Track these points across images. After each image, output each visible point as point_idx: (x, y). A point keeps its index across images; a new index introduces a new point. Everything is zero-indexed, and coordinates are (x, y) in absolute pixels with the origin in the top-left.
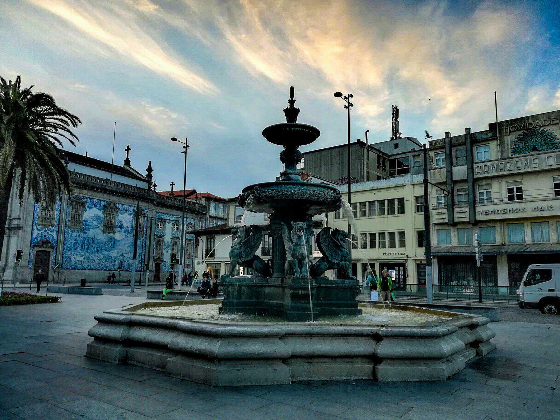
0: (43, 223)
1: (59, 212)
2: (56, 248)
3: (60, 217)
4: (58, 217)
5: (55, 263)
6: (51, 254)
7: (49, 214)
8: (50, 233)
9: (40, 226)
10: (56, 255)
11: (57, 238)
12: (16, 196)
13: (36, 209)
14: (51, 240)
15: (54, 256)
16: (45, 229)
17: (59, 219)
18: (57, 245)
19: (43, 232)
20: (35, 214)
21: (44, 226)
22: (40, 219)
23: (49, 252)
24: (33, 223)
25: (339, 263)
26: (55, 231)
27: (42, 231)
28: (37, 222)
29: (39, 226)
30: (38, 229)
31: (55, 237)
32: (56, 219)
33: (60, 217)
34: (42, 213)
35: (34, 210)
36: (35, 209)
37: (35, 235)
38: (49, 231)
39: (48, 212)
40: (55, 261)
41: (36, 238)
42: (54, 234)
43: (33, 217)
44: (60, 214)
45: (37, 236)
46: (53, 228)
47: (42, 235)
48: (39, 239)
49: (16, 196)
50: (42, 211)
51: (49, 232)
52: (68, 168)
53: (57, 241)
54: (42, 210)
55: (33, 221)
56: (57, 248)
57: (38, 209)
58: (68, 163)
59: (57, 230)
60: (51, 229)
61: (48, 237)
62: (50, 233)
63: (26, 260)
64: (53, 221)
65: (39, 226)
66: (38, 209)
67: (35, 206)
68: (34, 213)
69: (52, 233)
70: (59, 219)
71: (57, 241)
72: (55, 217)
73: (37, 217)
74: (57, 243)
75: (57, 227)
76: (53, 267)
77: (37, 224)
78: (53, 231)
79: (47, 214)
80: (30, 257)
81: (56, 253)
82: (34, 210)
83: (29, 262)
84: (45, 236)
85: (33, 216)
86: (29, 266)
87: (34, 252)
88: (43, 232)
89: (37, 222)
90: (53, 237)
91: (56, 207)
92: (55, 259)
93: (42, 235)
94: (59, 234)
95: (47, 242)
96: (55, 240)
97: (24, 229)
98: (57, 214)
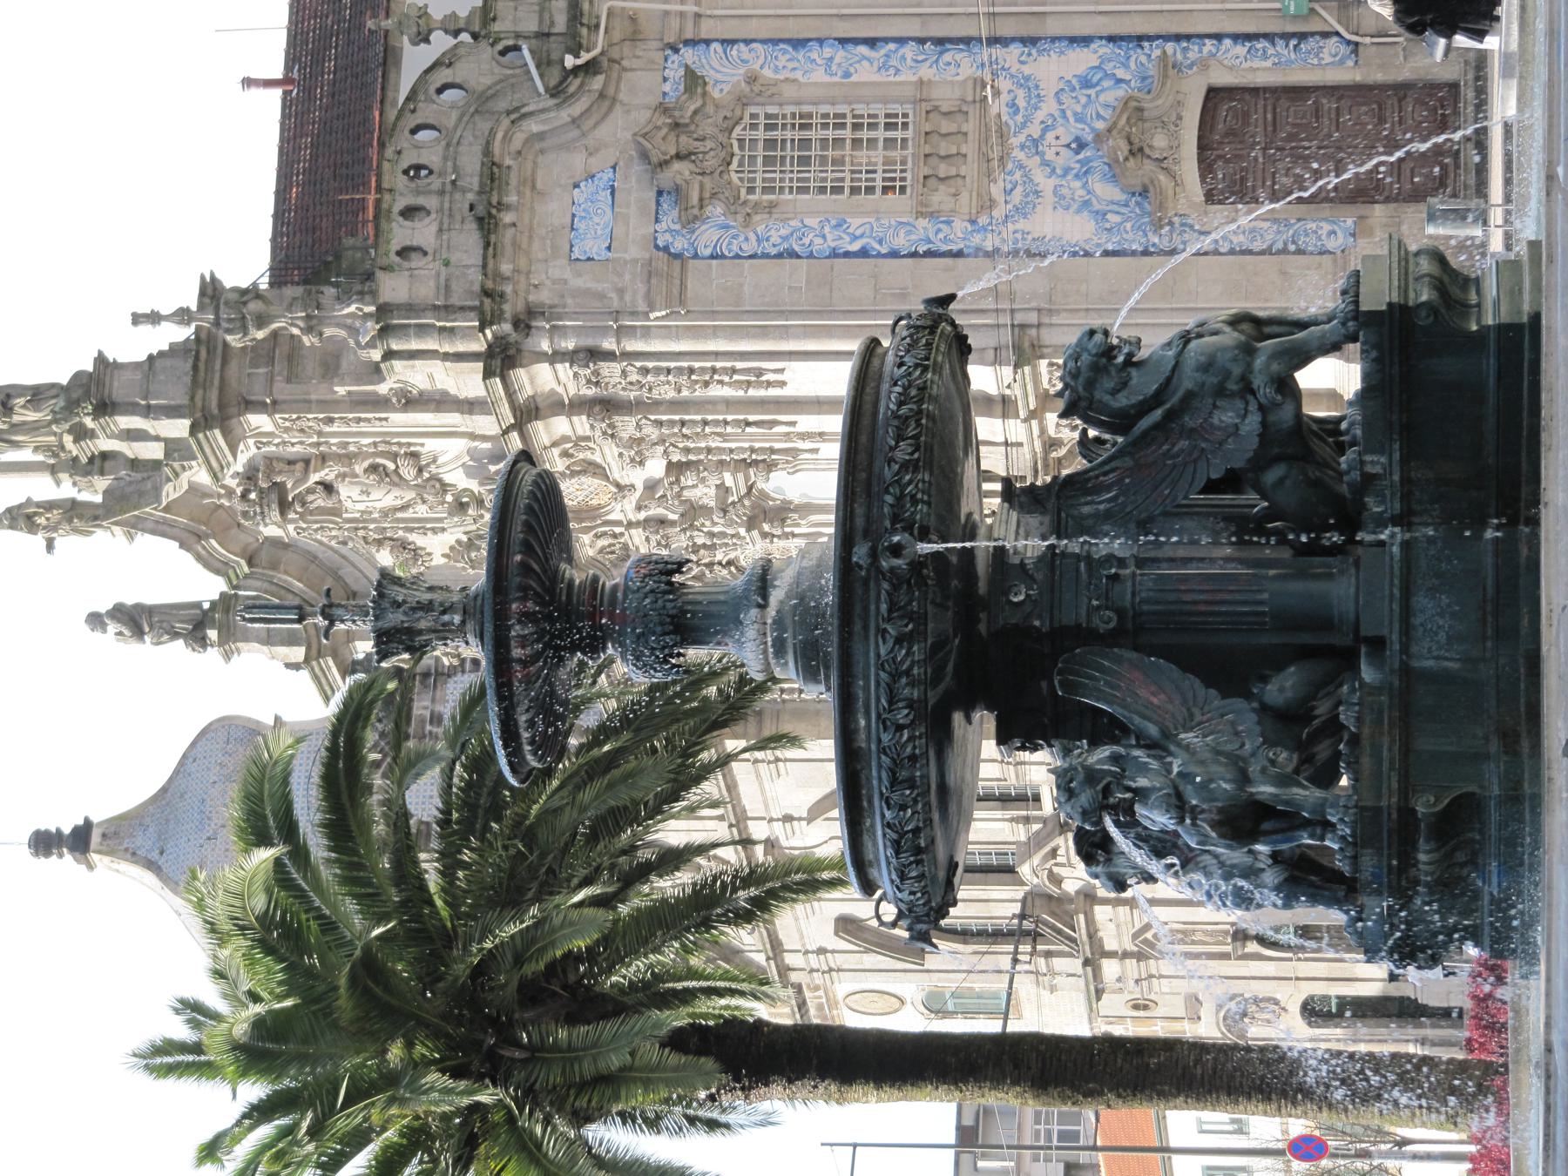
0: (970, 169)
1: (863, 49)
2: (1170, 47)
3: (901, 41)
4: (909, 50)
5: (1302, 36)
6: (1222, 78)
7: (888, 126)
8: (1049, 107)
9: (996, 191)
10: (1238, 38)
11: (1085, 41)
12: (769, 384)
13: (855, 238)
14: (1113, 95)
15: (1241, 50)
16: (1018, 154)
17: (921, 41)
18: (1150, 38)
19: (1045, 163)
20: (901, 242)
21: (995, 159)
22: (940, 197)
23: (1214, 95)
24: (979, 252)
25: (1261, 408)
26: (1027, 70)
27: (1039, 176)
28: (960, 226)
29: (992, 203)
30: (1022, 211)
31: (1082, 60)
32: (926, 72)
33: (901, 41)
34: (885, 190)
35: (864, 253)
36: (855, 247)
37: (1079, 229)
38: (1024, 125)
39: (872, 142)
40: (1286, 36)
41: (1101, 215)
42: (1054, 68)
43: (929, 254)
44: (872, 42)
45: (1086, 204)
46: (1004, 84)
47: (1067, 171)
48: (1106, 191)
49: (769, 384)
50: (870, 190)
51: (1040, 115)
52: (463, 13)
53: (1112, 39)
54: (855, 191)
55: (959, 254)
56: (1178, 38)
57: (855, 222)
58: (423, 13)
59: (1016, 50)
60: (1013, 105)
61: (1079, 118)
62: (1049, 107)
63: (1283, 273)
64: (946, 96)
65: (992, 203)
66: (855, 222)
67: (834, 254)
68: (894, 254)
69: (1049, 87)
70: (921, 41)
71: (1112, 39)
72: (907, 76)
73: (922, 222)
74: (1140, 39)
75: (997, 51)
76: (1344, 50)
77: (983, 220)
78: (1025, 82)
79: (890, 142)
80: (1257, 246)
81: (1218, 37)
82: (864, 253)
83: (1300, 252)
84: (1081, 145)
85: (914, 255)
86: (1331, 244)
87: (1219, 212)
88: (1045, 163)
89: (960, 226)
90: (1086, 83)
91: (819, 76)
92: (1269, 37)
93: (1067, 171)
94: (1053, 27)
95: (1134, 111)
96: (1103, 59)
97: (1032, 318)
98: (884, 67)
